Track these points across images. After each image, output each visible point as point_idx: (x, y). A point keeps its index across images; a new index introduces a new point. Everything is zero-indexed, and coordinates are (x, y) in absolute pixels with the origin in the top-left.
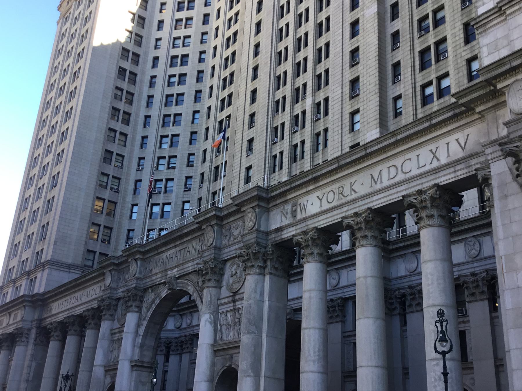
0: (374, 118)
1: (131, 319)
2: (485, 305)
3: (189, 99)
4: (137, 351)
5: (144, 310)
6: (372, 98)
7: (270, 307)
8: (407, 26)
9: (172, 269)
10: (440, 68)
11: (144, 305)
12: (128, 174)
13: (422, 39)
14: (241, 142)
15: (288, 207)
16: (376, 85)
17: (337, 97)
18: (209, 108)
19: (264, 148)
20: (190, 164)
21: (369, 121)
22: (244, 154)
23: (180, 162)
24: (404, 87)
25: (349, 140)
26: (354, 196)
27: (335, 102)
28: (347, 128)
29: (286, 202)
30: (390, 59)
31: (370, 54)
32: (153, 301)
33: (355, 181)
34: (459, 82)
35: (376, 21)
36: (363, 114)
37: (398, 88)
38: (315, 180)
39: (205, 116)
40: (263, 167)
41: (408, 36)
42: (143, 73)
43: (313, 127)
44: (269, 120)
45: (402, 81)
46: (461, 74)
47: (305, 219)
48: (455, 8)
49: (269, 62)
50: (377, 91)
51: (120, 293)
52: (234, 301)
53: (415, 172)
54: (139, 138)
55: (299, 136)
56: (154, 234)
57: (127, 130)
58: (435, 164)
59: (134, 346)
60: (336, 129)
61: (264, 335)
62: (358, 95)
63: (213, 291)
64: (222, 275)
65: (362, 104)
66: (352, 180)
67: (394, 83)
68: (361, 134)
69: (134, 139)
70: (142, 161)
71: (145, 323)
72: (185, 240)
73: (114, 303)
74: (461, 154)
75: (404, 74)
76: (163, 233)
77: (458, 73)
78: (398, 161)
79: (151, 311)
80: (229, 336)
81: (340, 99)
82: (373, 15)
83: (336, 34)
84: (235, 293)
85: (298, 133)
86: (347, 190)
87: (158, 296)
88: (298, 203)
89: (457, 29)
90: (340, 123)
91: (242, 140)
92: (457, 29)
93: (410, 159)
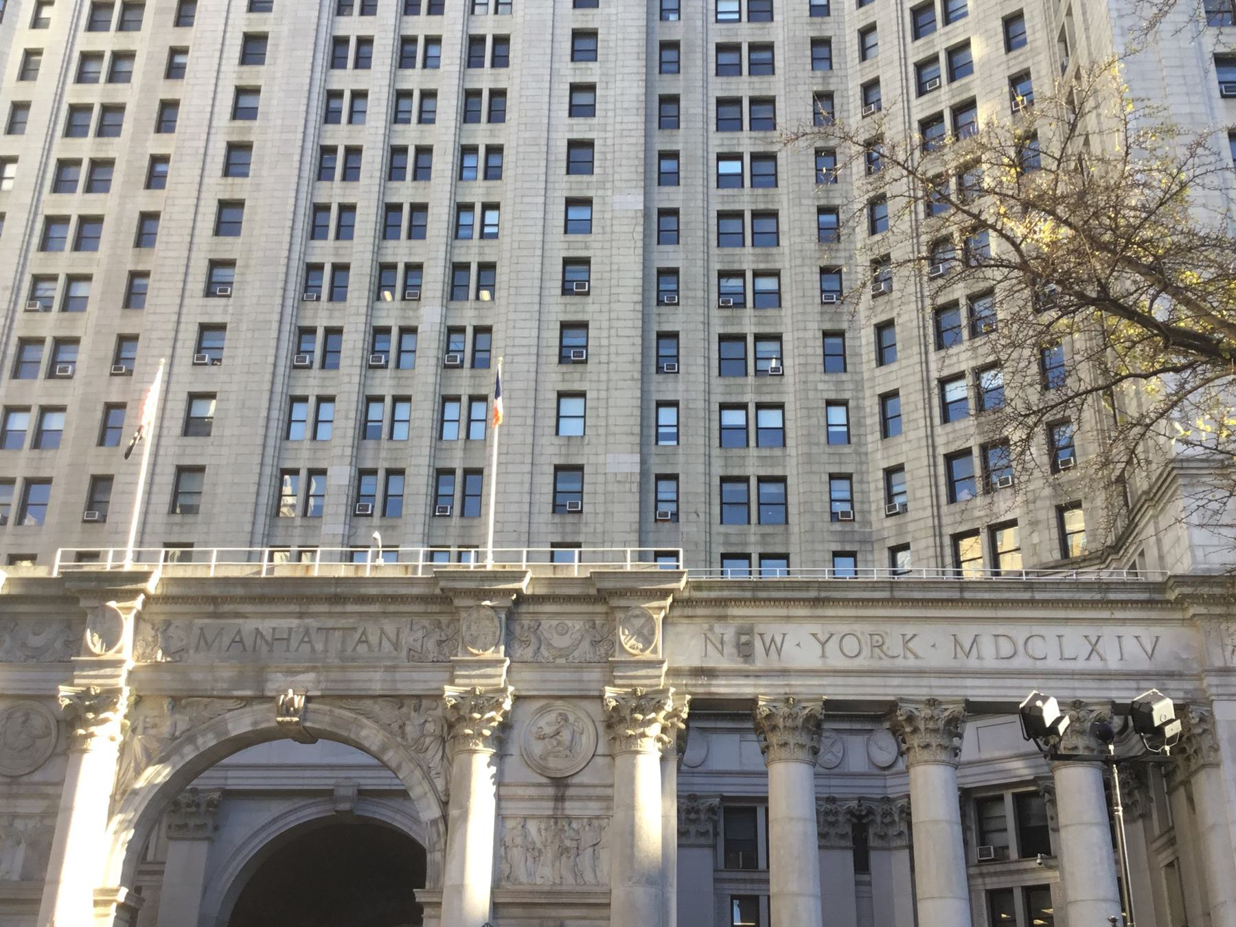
0: (627, 429)
2: (849, 856)
6: (621, 384)
8: (698, 270)
10: (765, 389)
13: (727, 312)
14: (175, 318)
16: (634, 362)
17: (525, 342)
19: (270, 369)
21: (612, 429)
24: (687, 391)
25: (550, 450)
26: (911, 663)
27: (517, 351)
29: (722, 618)
30: (654, 318)
31: (620, 290)
33: (914, 636)
34: (809, 435)
35: (640, 229)
36: (597, 408)
37: (671, 386)
38: (817, 602)
40: (264, 414)
41: (700, 294)
44: (289, 302)
45: (680, 376)
46: (814, 421)
47: (784, 673)
48: (809, 293)
49: (297, 158)
50: (637, 376)
53: (1053, 663)
55: (389, 382)
58: (1095, 664)
60: (521, 412)
62: (586, 362)
65: (594, 385)
66: (909, 630)
68: (586, 450)
72: (350, 608)
75: (688, 365)
77: (809, 417)
78: (1020, 633)
81: (534, 350)
82: (632, 214)
83: (526, 200)
85: (388, 373)
88: (756, 631)
89: (809, 334)
90: (531, 404)
91: (179, 314)
92: (809, 334)
93: (1042, 637)
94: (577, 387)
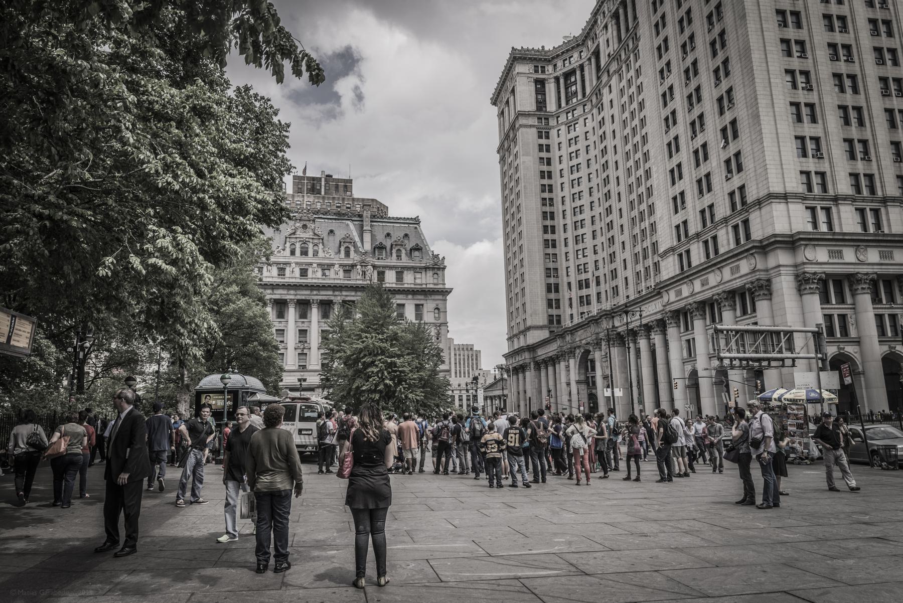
1: (572, 362)
3: (587, 208)
20: (595, 252)
23: (589, 252)
42: (557, 196)
43: (651, 239)
54: (563, 240)
57: (555, 237)
69: (560, 242)
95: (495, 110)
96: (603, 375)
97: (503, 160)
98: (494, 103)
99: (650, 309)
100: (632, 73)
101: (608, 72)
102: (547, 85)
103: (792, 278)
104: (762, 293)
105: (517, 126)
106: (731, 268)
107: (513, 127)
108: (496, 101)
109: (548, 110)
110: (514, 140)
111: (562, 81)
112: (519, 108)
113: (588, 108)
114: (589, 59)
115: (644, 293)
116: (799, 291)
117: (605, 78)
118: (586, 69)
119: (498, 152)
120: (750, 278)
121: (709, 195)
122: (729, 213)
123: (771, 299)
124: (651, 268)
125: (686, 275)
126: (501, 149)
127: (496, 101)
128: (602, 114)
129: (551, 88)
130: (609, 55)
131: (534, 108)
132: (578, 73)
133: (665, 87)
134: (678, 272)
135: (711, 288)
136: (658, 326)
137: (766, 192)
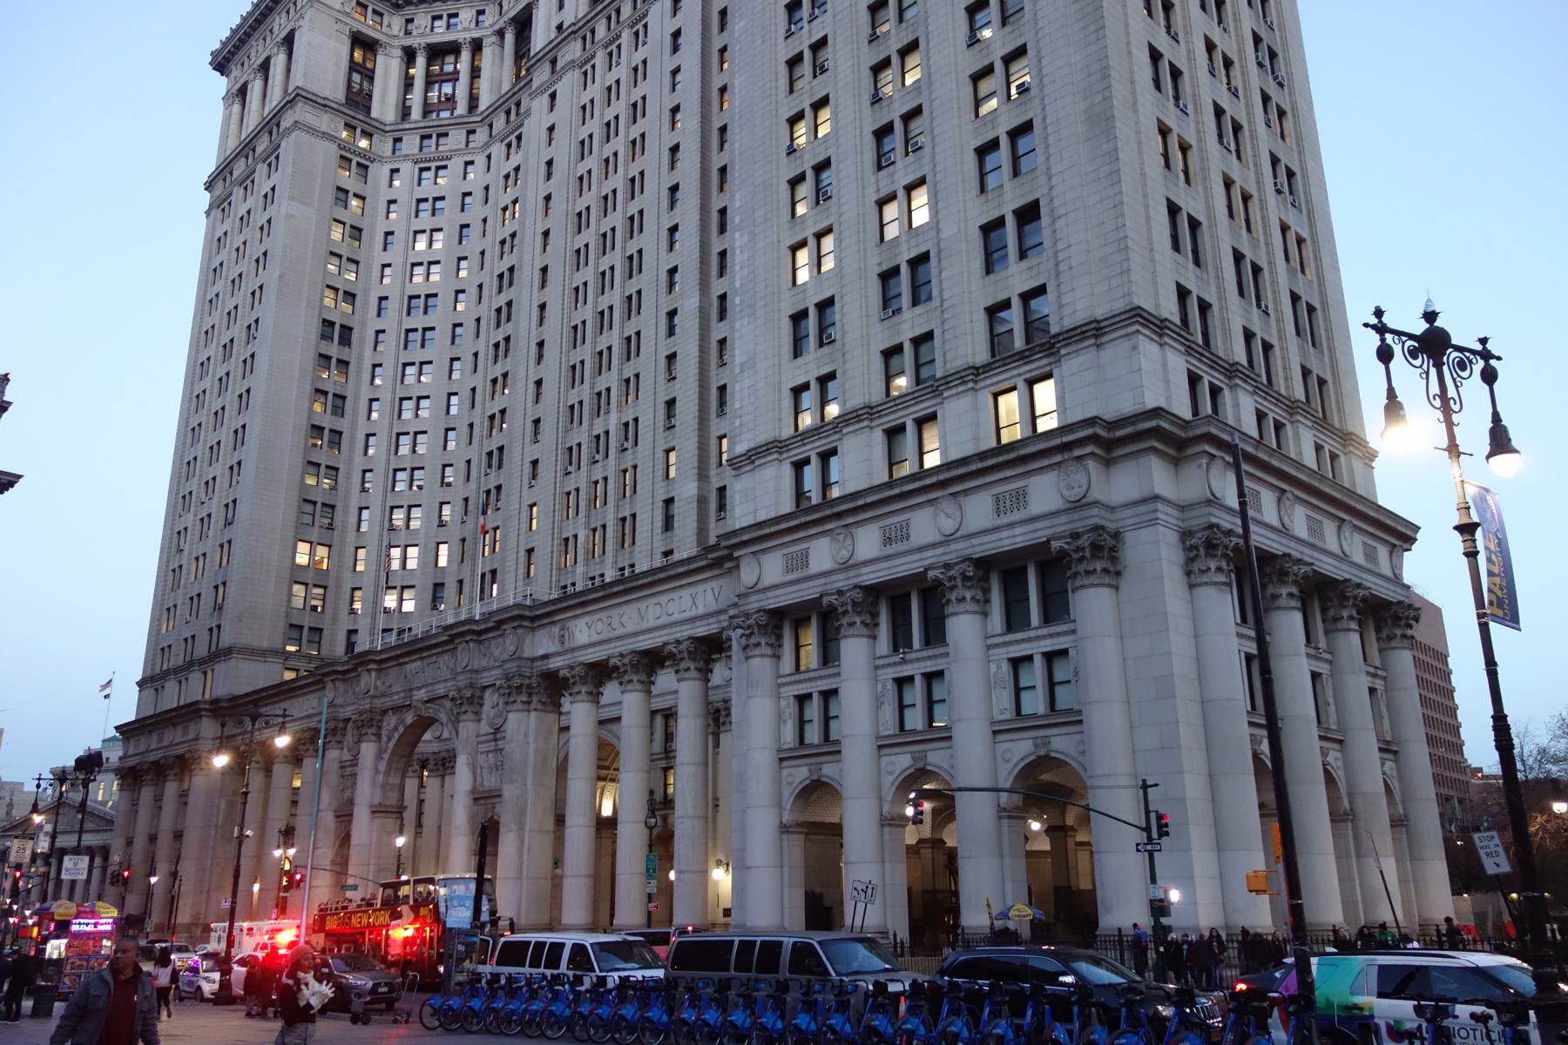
1: (368, 750)
4: (378, 793)
5: (384, 738)
7: (536, 751)
9: (419, 688)
11: (384, 732)
12: (347, 497)
15: (556, 629)
18: (474, 390)
22: (526, 482)
28: (660, 472)
29: (553, 623)
32: (396, 728)
39: (468, 403)
47: (573, 650)
51: (347, 712)
52: (496, 740)
53: (677, 617)
56: (392, 638)
57: (343, 424)
58: (693, 613)
59: (373, 785)
61: (529, 783)
63: (471, 725)
64: (481, 705)
67: (719, 416)
69: (353, 439)
70: (368, 475)
71: (386, 756)
73: (341, 725)
74: (713, 607)
76: (406, 637)
78: (663, 599)
79: (394, 741)
80: (490, 782)
84: (497, 730)
86: (616, 624)
87: (402, 721)
94: (670, 445)
95: (220, 84)
96: (473, 791)
97: (219, 206)
98: (221, 63)
99: (672, 608)
100: (622, 72)
101: (554, 62)
102: (380, 58)
103: (1173, 537)
104: (1099, 566)
105: (285, 124)
106: (997, 498)
107: (271, 125)
108: (227, 60)
109: (374, 114)
110: (272, 158)
111: (421, 61)
112: (297, 80)
113: (481, 136)
114: (501, 34)
115: (579, 588)
116: (1188, 573)
117: (541, 75)
118: (488, 52)
119: (209, 186)
120: (1062, 525)
121: (919, 310)
122: (982, 355)
123: (1117, 588)
124: (610, 530)
125: (816, 514)
126: (224, 182)
127: (227, 60)
128: (515, 159)
129: (388, 68)
130: (560, 27)
131: (340, 95)
132: (465, 55)
133: (803, 42)
134: (787, 506)
135: (921, 549)
136: (693, 655)
137: (1119, 305)
